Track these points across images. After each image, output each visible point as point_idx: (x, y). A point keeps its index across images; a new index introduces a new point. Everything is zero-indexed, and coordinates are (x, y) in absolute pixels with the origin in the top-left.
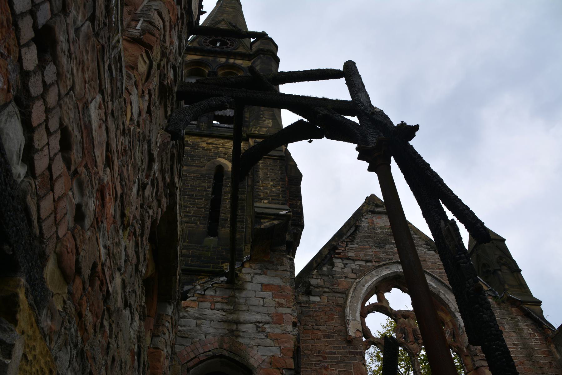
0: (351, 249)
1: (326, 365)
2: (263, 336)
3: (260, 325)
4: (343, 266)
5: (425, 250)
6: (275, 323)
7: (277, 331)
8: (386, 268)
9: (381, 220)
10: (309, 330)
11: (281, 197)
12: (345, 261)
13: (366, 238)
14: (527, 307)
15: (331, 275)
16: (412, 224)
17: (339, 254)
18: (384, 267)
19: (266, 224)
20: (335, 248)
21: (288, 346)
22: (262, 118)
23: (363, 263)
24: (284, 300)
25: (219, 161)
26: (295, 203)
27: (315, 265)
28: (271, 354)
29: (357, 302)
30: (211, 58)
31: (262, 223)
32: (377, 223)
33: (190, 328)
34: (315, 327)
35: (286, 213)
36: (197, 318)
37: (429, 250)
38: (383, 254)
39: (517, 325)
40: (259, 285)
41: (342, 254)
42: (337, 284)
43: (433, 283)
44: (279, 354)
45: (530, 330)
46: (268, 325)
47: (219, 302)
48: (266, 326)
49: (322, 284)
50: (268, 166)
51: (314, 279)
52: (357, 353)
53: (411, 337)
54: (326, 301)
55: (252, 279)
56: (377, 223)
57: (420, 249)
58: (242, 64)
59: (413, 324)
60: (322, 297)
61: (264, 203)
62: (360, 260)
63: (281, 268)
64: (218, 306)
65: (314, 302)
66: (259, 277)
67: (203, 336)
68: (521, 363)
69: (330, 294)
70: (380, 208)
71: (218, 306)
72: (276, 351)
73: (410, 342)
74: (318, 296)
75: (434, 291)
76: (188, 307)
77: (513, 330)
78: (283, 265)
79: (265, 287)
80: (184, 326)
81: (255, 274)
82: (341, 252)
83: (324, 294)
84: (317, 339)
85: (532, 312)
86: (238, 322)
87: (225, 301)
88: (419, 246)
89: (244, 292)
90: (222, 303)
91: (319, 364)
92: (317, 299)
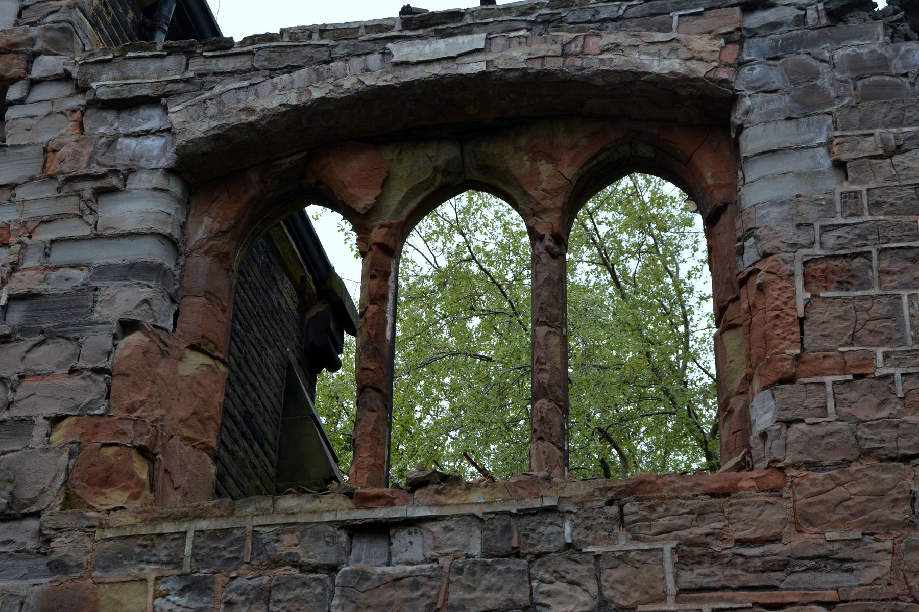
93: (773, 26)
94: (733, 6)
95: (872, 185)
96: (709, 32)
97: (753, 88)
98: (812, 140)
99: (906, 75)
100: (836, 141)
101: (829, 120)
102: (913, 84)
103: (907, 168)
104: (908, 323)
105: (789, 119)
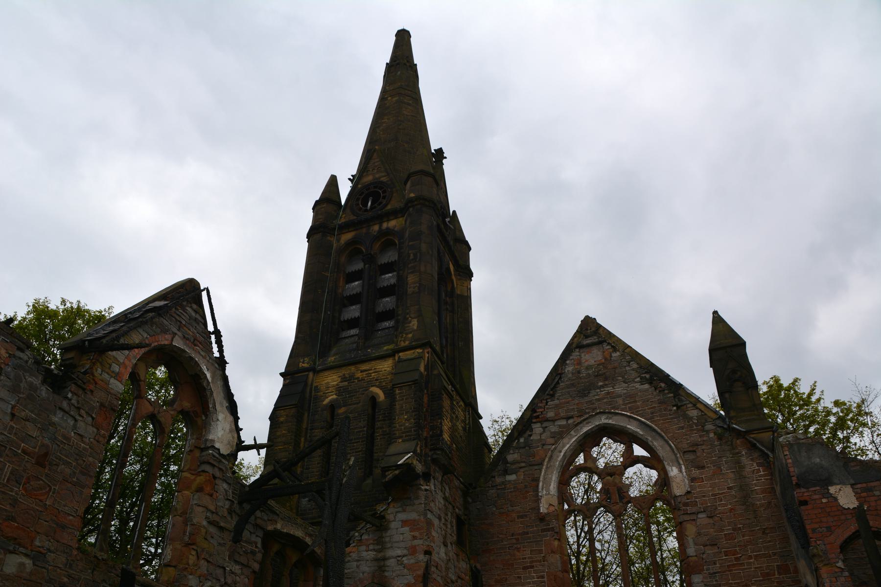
1: (519, 546)
2: (401, 567)
3: (399, 559)
4: (542, 430)
5: (638, 386)
6: (410, 555)
7: (412, 561)
8: (587, 423)
10: (503, 513)
11: (413, 431)
12: (544, 425)
14: (753, 438)
15: (527, 444)
16: (631, 347)
17: (537, 417)
18: (585, 422)
19: (390, 475)
20: (534, 411)
21: (419, 573)
22: (408, 318)
23: (564, 422)
24: (417, 533)
25: (372, 391)
27: (516, 434)
28: (406, 582)
29: (552, 473)
30: (364, 230)
31: (386, 476)
32: (586, 361)
33: (352, 570)
34: (510, 508)
35: (404, 461)
36: (358, 561)
38: (586, 404)
39: (738, 462)
40: (400, 523)
41: (540, 417)
43: (640, 429)
44: (413, 581)
45: (755, 464)
46: (406, 557)
47: (372, 544)
48: (404, 559)
49: (519, 458)
50: (404, 396)
51: (511, 455)
52: (548, 530)
53: (616, 497)
54: (522, 477)
55: (395, 518)
56: (586, 361)
57: (632, 385)
58: (396, 226)
59: (617, 482)
60: (519, 473)
61: (399, 442)
62: (560, 419)
63: (417, 502)
64: (371, 547)
65: (509, 481)
66: (400, 515)
67: (361, 574)
68: (732, 509)
69: (527, 469)
70: (590, 338)
71: (371, 547)
72: (410, 579)
73: (613, 504)
74: (515, 473)
75: (643, 438)
76: (350, 552)
77: (731, 469)
78: (419, 499)
79: (405, 523)
80: (349, 569)
81: (397, 512)
82: (539, 415)
83: (522, 470)
84: (511, 521)
85: (758, 442)
86: (385, 559)
87: (375, 542)
88: (630, 382)
89: (389, 532)
90: (374, 544)
91: (512, 547)
92: (513, 477)
93: (20, 358)
94: (16, 346)
95: (18, 427)
96: (6, 350)
97: (5, 374)
98: (10, 401)
99: (39, 397)
100: (17, 408)
101: (17, 398)
102: (39, 400)
103: (27, 427)
104: (4, 473)
105: (8, 391)
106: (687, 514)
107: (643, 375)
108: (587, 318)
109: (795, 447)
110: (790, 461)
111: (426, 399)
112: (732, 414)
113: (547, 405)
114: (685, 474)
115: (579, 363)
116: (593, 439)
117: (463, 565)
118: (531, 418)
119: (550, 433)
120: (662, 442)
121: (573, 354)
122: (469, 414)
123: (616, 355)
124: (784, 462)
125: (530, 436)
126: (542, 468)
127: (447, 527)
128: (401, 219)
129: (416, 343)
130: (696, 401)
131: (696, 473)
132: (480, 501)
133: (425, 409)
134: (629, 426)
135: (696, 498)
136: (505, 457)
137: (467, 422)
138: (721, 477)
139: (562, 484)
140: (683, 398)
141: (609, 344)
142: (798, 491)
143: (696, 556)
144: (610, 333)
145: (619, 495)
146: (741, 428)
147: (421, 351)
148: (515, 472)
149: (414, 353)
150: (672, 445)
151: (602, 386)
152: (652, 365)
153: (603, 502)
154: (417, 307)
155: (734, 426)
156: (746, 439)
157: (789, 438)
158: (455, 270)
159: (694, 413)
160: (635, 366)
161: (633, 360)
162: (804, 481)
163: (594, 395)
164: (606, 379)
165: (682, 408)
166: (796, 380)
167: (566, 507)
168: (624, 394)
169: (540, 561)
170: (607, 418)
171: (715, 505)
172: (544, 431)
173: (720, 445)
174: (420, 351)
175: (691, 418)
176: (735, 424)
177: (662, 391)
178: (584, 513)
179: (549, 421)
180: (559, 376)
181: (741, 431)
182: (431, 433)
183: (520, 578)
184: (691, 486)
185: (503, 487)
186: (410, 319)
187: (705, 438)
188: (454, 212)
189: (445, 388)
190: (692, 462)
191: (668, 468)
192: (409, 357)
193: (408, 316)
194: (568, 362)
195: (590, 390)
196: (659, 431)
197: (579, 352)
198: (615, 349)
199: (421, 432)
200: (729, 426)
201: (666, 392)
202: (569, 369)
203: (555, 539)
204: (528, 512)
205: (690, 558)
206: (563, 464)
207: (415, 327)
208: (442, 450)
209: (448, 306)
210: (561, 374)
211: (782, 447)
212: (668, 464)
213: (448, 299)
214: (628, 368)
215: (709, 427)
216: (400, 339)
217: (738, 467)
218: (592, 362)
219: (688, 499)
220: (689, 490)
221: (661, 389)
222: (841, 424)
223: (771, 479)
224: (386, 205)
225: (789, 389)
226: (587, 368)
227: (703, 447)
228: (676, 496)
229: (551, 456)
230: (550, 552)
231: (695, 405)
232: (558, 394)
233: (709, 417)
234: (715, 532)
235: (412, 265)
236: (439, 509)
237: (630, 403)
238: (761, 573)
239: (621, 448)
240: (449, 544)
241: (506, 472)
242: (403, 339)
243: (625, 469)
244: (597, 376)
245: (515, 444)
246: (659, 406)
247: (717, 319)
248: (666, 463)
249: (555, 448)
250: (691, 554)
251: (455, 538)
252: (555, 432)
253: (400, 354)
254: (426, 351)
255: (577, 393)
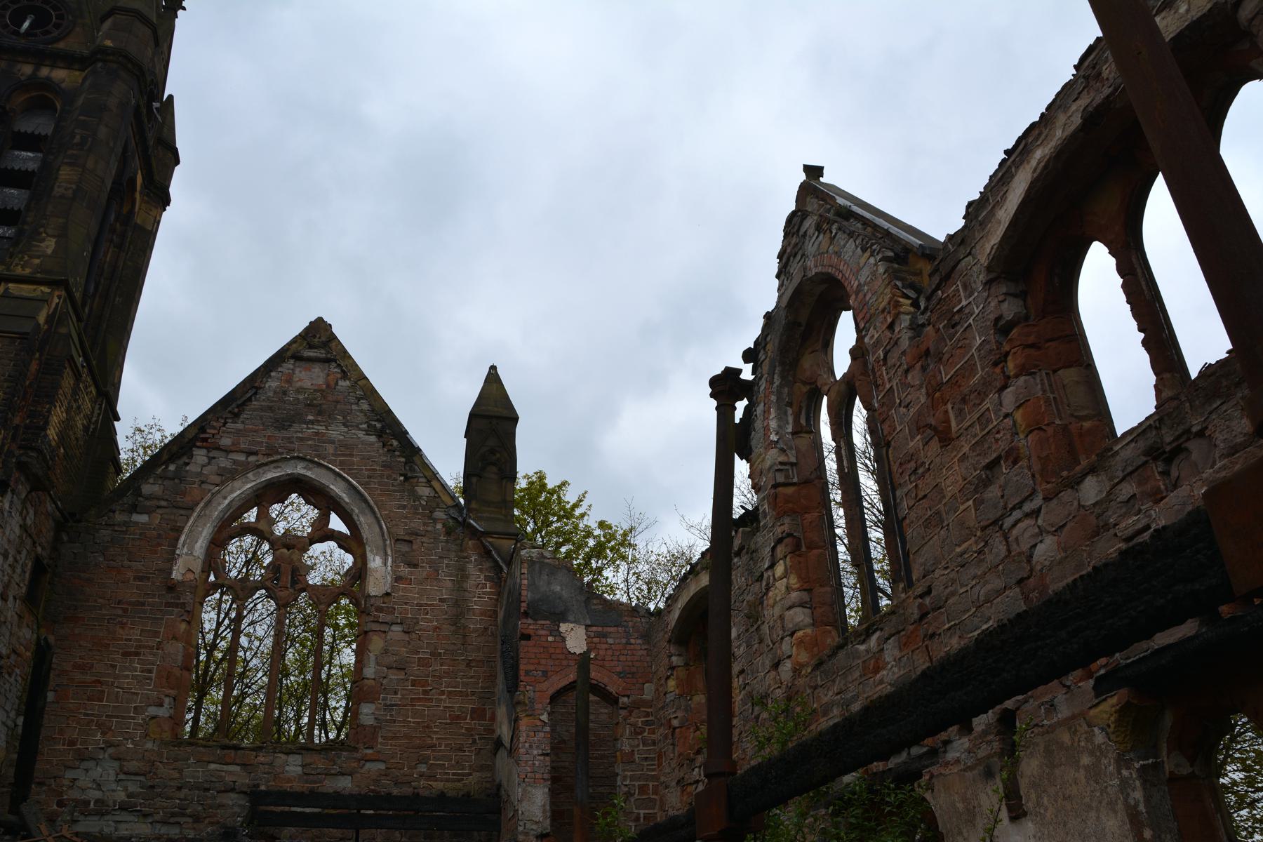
0: (231, 432)
1: (125, 621)
5: (361, 434)
8: (275, 468)
9: (308, 373)
12: (211, 455)
13: (262, 411)
14: (489, 542)
15: (179, 476)
17: (205, 440)
18: (273, 465)
20: (203, 430)
22: (41, 233)
23: (242, 458)
26: (39, 409)
27: (165, 457)
29: (205, 525)
32: (301, 380)
34: (126, 563)
37: (367, 435)
39: (463, 569)
41: (209, 441)
42: (184, 494)
45: (482, 577)
49: (160, 493)
51: (149, 485)
52: (177, 606)
53: (287, 579)
56: (301, 380)
57: (353, 431)
58: (64, 81)
59: (295, 559)
65: (136, 523)
68: (438, 628)
69: (167, 510)
74: (147, 513)
75: (347, 507)
82: (209, 438)
83: (160, 511)
85: (495, 549)
92: (143, 518)
106: (378, 622)
107: (373, 423)
108: (320, 320)
109: (537, 566)
110: (525, 582)
111: (34, 367)
112: (474, 505)
113: (224, 426)
114: (389, 568)
115: (289, 381)
116: (278, 491)
117: (27, 634)
118: (196, 438)
119: (216, 467)
120: (371, 520)
121: (285, 365)
122: (100, 409)
123: (344, 384)
124: (518, 581)
125: (187, 464)
126: (191, 515)
127: (14, 572)
128: (77, 73)
129: (43, 276)
130: (432, 476)
131: (404, 570)
132: (82, 543)
133: (28, 383)
134: (332, 487)
135: (395, 603)
136: (139, 489)
137: (94, 419)
138: (435, 583)
139: (213, 543)
140: (416, 467)
141: (339, 366)
142: (525, 621)
143: (374, 679)
144: (345, 351)
145: (292, 578)
146: (480, 526)
147: (49, 290)
148: (148, 511)
149: (35, 290)
150: (384, 527)
151: (312, 422)
152: (390, 412)
153: (267, 583)
154: (61, 220)
155: (472, 521)
156: (482, 543)
157: (533, 553)
158: (144, 186)
159: (424, 491)
160: (365, 407)
161: (365, 397)
162: (533, 612)
163: (296, 431)
164: (320, 413)
165: (412, 480)
166: (564, 484)
167: (212, 578)
168: (339, 441)
169: (152, 648)
170: (305, 468)
171: (418, 619)
172: (209, 463)
173: (447, 542)
174: (46, 289)
175: (419, 498)
176: (473, 520)
177: (391, 451)
178: (236, 591)
179: (221, 450)
180: (254, 390)
181: (477, 529)
182: (28, 421)
183: (114, 666)
184: (393, 587)
185: (124, 529)
186: (44, 235)
187: (429, 529)
188: (171, 97)
189: (71, 360)
190: (403, 555)
191: (370, 556)
192: (25, 294)
193: (42, 230)
194: (273, 374)
195: (294, 422)
196: (372, 503)
197: (293, 364)
198: (345, 375)
199: (10, 415)
200: (464, 520)
201: (397, 453)
202: (272, 384)
203: (184, 620)
204: (152, 574)
205: (366, 680)
206: (224, 516)
207: (49, 251)
208: (40, 452)
209: (115, 237)
210: (258, 388)
211: (522, 563)
212: (371, 551)
213: (118, 225)
214: (354, 407)
215: (439, 514)
216: (16, 261)
217: (461, 576)
218: (307, 384)
219: (384, 603)
220: (389, 591)
221: (390, 448)
222: (599, 551)
223: (497, 600)
224: (57, 40)
225: (552, 492)
226: (300, 390)
227: (424, 539)
228: (369, 596)
229: (210, 501)
230: (171, 637)
231: (429, 481)
232: (245, 416)
233: (443, 502)
234: (407, 653)
235: (75, 152)
236: (9, 541)
237: (343, 455)
238: (450, 715)
239: (314, 513)
240: (11, 598)
241: (134, 508)
242: (22, 263)
243: (311, 544)
244: (309, 405)
245: (159, 470)
246: (382, 471)
247: (493, 377)
248: (368, 549)
249: (219, 492)
250: (368, 676)
251: (24, 590)
252: (224, 469)
253: (10, 285)
254: (57, 293)
255: (273, 421)
